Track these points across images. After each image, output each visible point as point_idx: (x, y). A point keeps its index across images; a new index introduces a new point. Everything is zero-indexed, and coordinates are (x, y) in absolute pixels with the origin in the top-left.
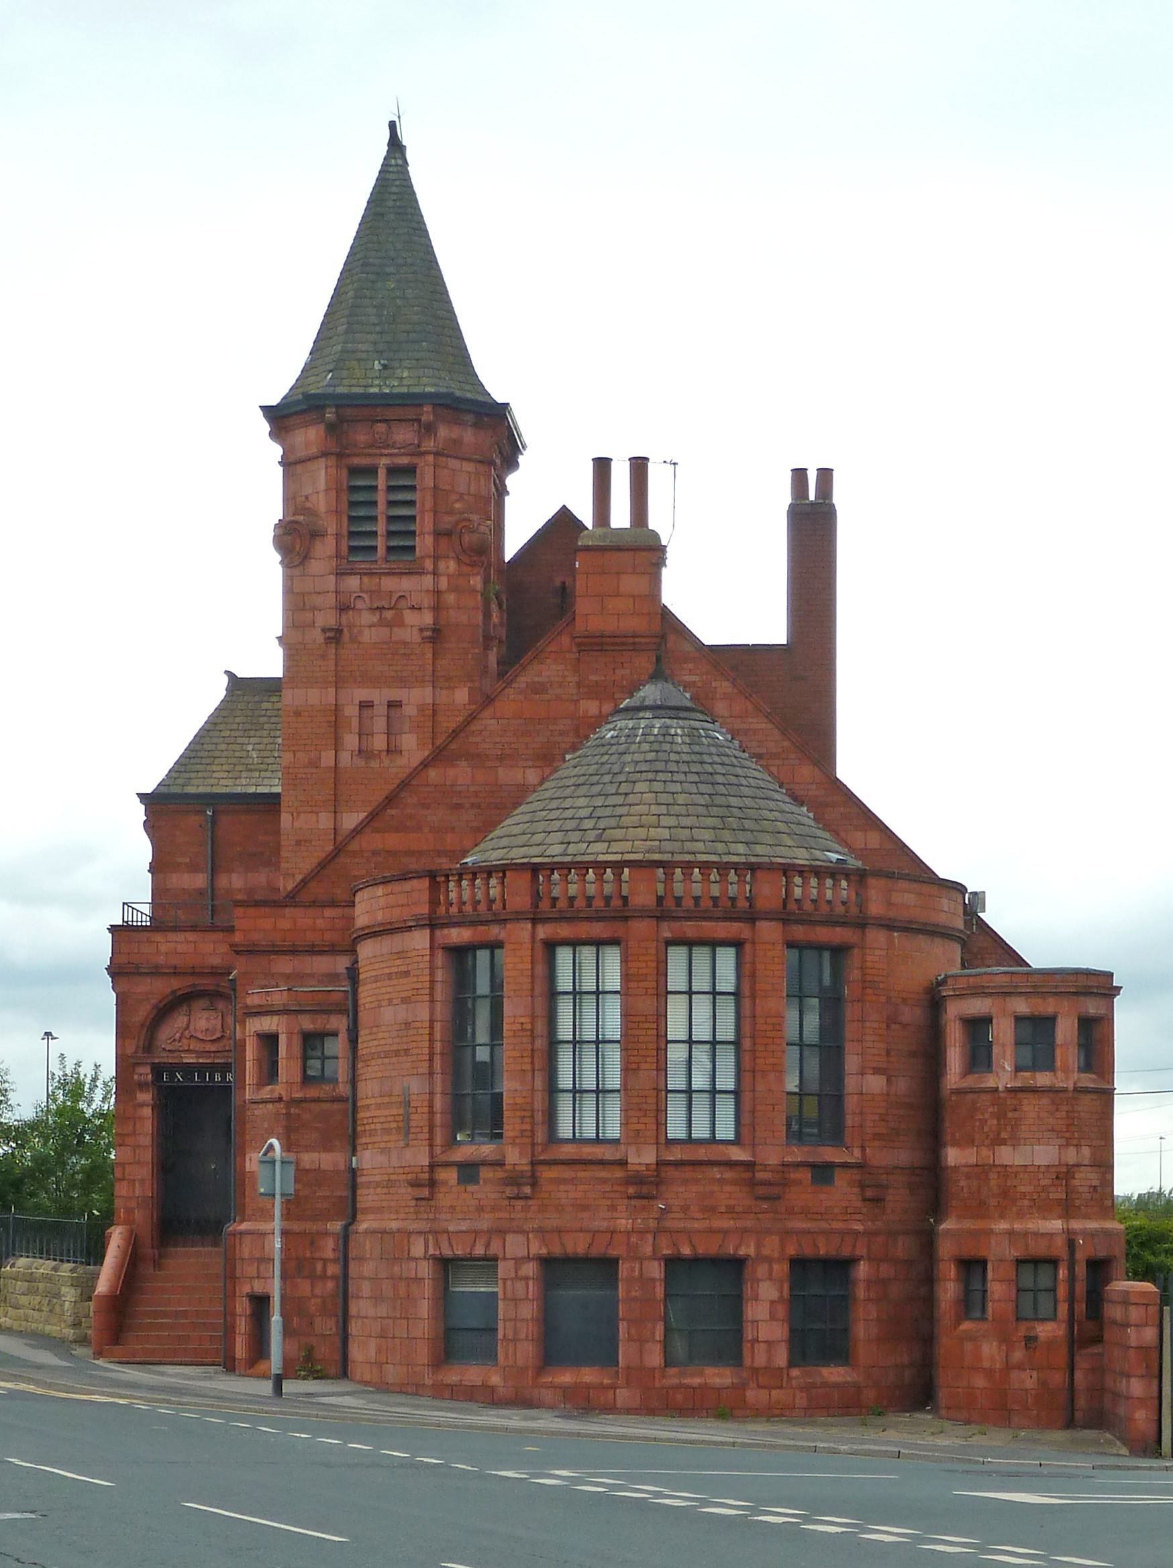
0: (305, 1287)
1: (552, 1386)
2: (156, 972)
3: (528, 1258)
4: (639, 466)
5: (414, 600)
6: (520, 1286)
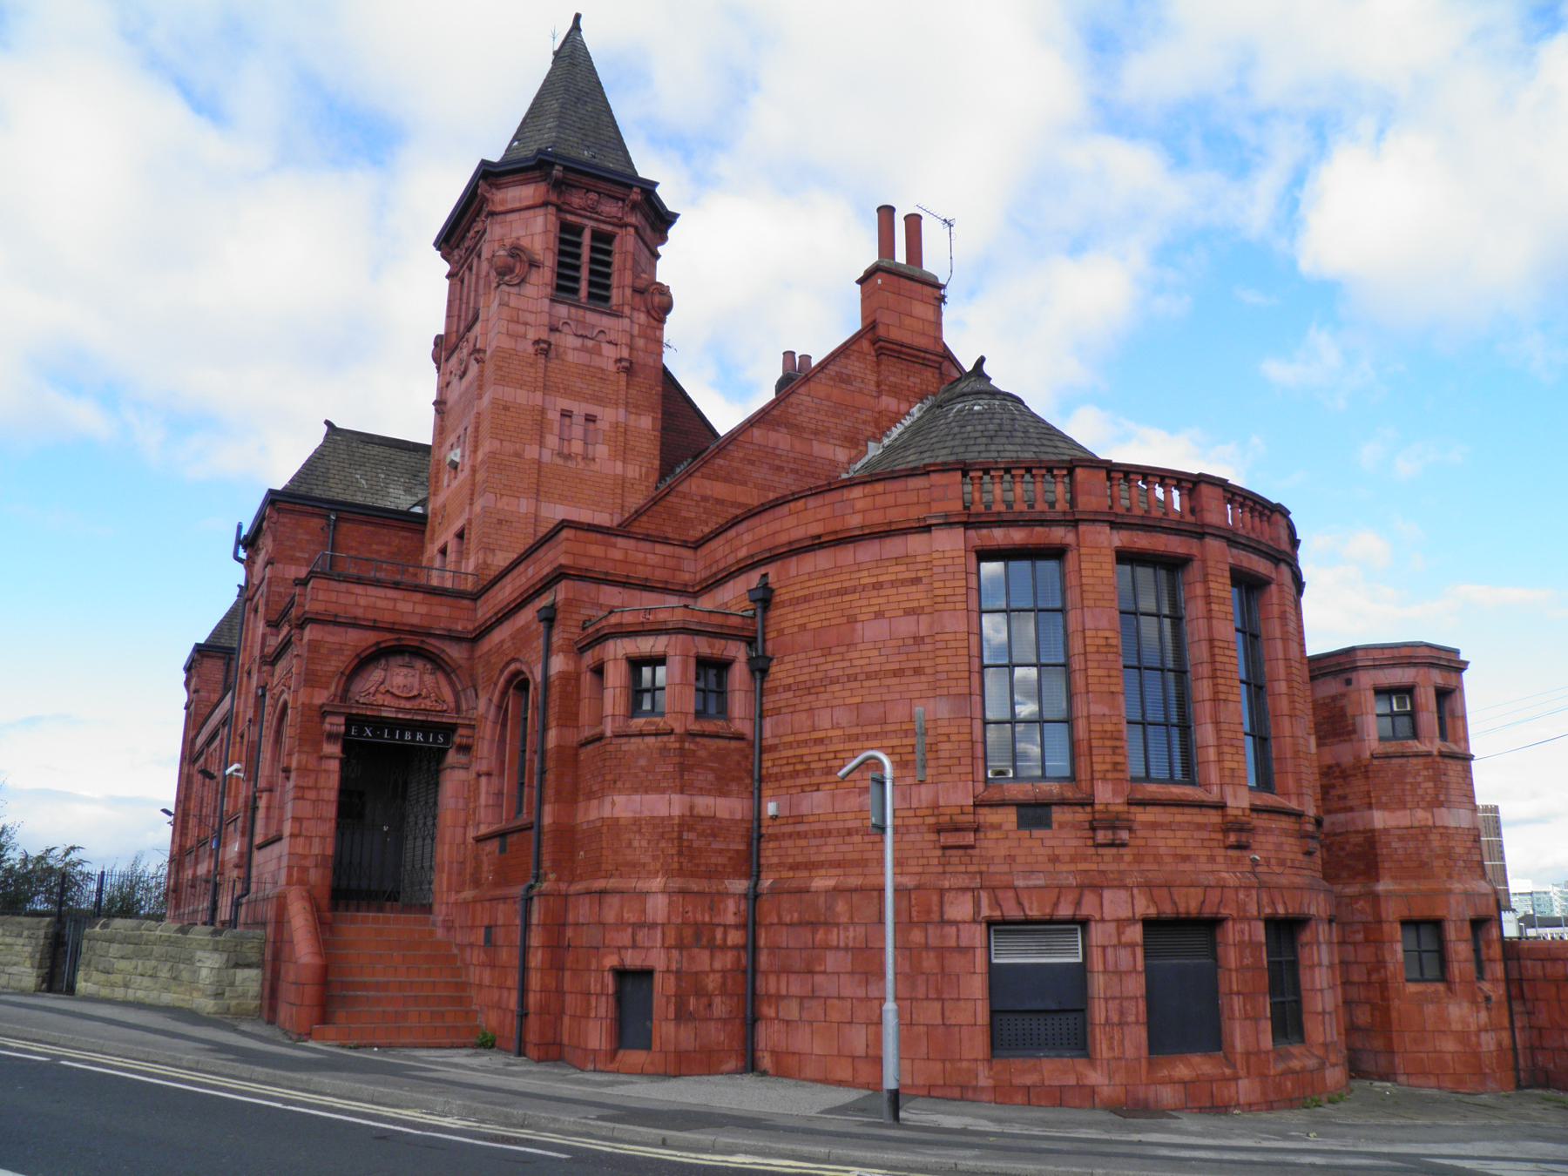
0: (703, 960)
1: (1171, 1081)
2: (354, 624)
3: (1131, 921)
4: (914, 222)
5: (613, 336)
6: (1124, 954)
